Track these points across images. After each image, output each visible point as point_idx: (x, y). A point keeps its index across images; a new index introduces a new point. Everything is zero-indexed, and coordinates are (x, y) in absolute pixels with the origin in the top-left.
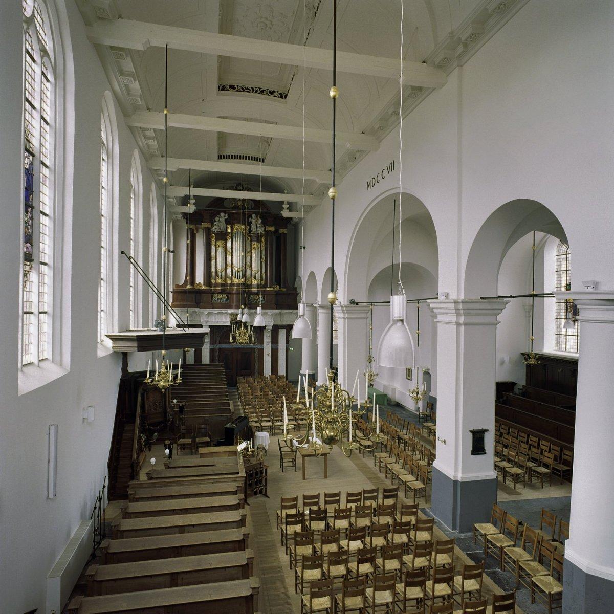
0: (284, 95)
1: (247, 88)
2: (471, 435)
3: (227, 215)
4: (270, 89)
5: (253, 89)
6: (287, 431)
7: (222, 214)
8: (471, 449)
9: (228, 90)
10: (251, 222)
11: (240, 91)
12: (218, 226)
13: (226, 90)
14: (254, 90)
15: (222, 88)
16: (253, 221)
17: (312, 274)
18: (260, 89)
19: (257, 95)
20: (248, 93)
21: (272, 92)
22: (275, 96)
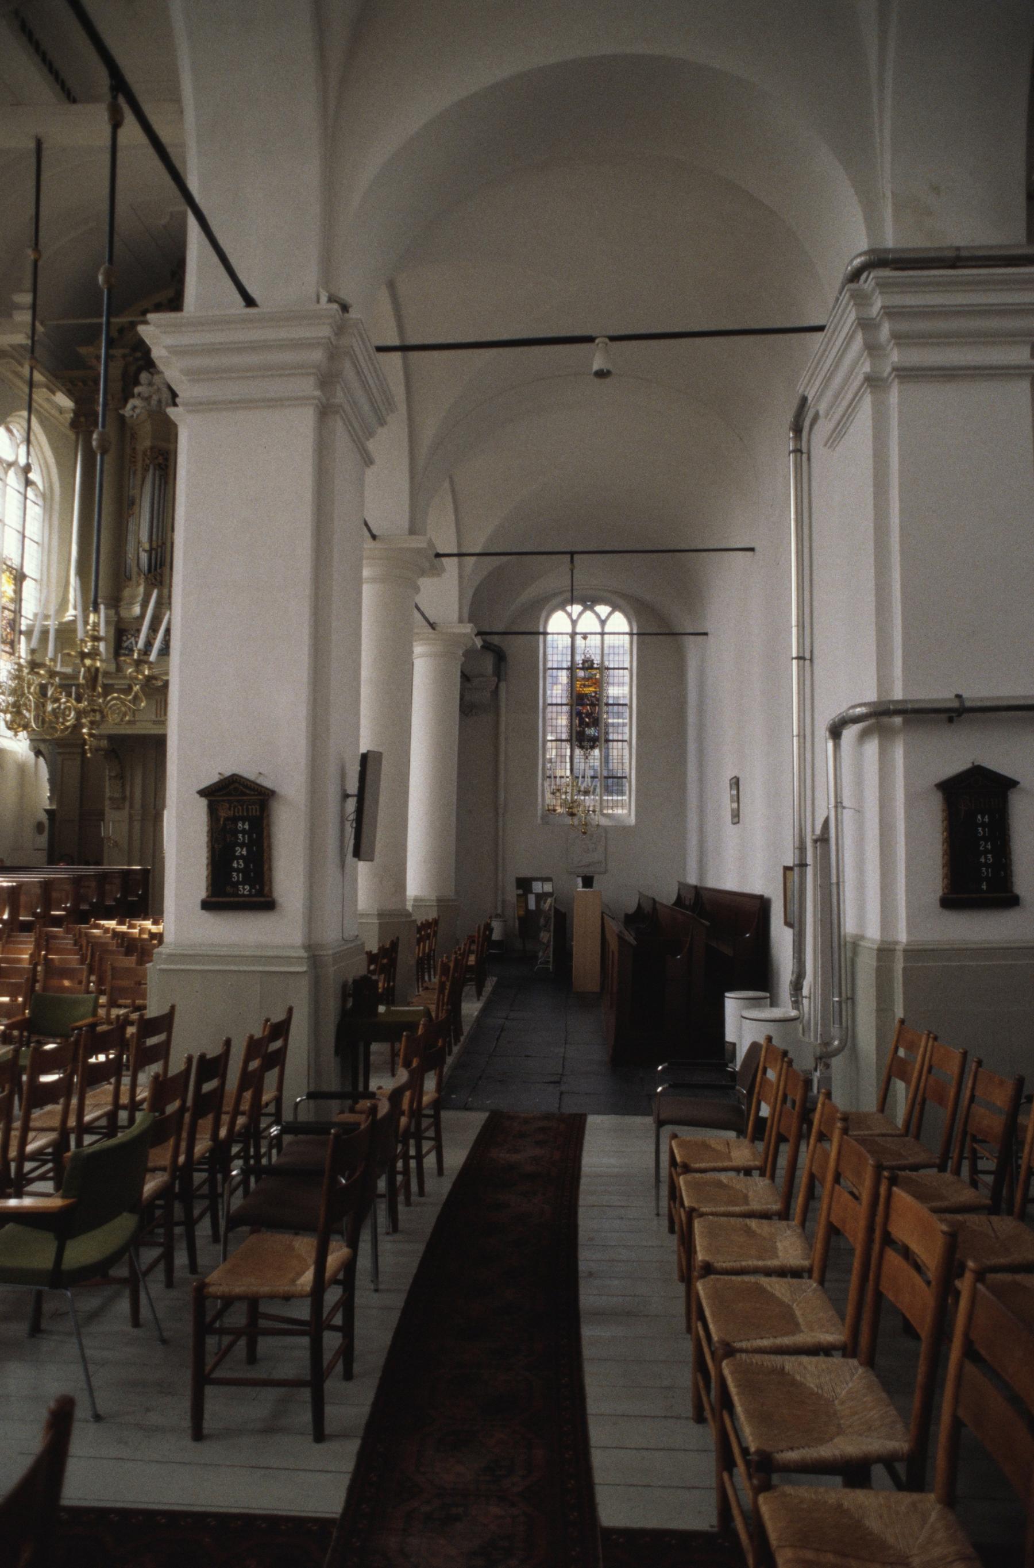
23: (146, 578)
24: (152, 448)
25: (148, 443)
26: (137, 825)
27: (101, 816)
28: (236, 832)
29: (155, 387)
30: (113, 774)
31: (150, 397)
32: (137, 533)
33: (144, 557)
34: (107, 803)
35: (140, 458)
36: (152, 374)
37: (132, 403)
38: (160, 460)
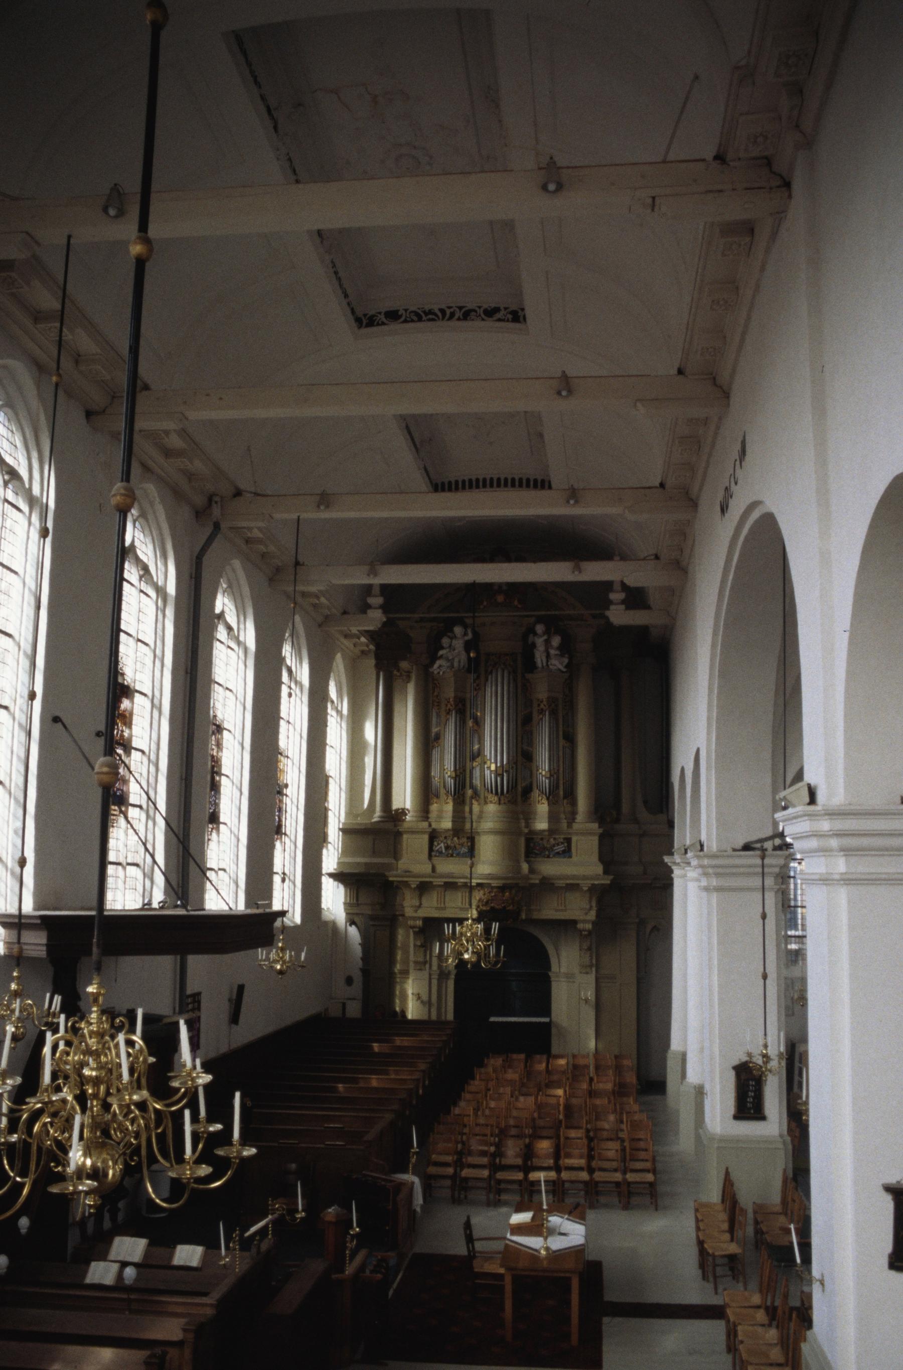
0: (520, 313)
1: (430, 312)
2: (887, 1204)
3: (469, 632)
4: (485, 306)
5: (443, 311)
6: (55, 1076)
7: (458, 630)
8: (887, 1244)
9: (383, 324)
10: (534, 645)
11: (412, 321)
12: (448, 660)
13: (378, 324)
14: (446, 314)
15: (365, 321)
16: (540, 642)
17: (683, 769)
18: (460, 308)
19: (454, 323)
20: (430, 324)
21: (490, 313)
22: (499, 320)
23: (454, 800)
26: (435, 982)
28: (748, 1086)
30: (419, 943)
31: (453, 659)
32: (442, 759)
33: (450, 782)
34: (412, 964)
36: (451, 638)
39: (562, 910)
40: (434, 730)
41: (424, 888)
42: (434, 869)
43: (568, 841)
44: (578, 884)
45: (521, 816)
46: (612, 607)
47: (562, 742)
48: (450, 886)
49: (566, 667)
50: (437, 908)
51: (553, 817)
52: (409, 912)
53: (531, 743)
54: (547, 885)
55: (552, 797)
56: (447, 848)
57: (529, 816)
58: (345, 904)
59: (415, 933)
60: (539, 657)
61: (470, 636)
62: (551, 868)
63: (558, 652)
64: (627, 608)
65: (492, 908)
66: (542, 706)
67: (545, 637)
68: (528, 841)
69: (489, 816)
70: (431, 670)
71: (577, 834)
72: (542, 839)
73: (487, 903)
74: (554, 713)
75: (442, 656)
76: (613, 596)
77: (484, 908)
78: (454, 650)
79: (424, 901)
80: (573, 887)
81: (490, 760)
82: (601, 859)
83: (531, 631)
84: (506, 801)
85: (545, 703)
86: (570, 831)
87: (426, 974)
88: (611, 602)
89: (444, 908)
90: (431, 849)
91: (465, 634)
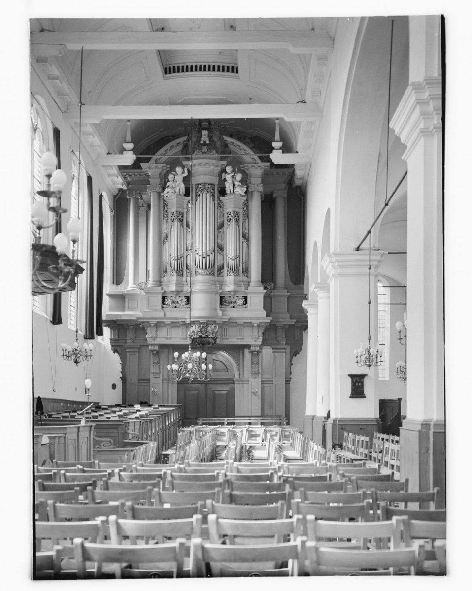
7: (179, 170)
10: (225, 180)
16: (228, 177)
24: (177, 211)
25: (175, 209)
27: (148, 380)
29: (178, 183)
32: (170, 248)
35: (170, 215)
37: (166, 190)
38: (180, 217)
39: (242, 339)
40: (165, 231)
41: (158, 325)
42: (165, 315)
43: (246, 298)
44: (251, 322)
45: (218, 283)
46: (274, 151)
47: (242, 239)
48: (174, 324)
49: (246, 192)
50: (167, 339)
51: (236, 283)
52: (150, 341)
53: (223, 240)
54: (232, 323)
55: (236, 270)
56: (173, 302)
57: (222, 284)
58: (111, 339)
59: (153, 354)
60: (228, 186)
61: (186, 174)
62: (233, 313)
63: (240, 184)
64: (283, 153)
65: (200, 336)
66: (230, 217)
67: (232, 174)
68: (222, 298)
69: (199, 283)
70: (162, 194)
71: (250, 293)
72: (230, 297)
73: (197, 333)
74: (237, 221)
75: (169, 186)
76: (274, 144)
77: (195, 337)
78: (176, 182)
79: (158, 332)
80: (249, 324)
81: (199, 249)
82: (265, 308)
83: (224, 171)
84: (208, 273)
85: (232, 215)
86: (247, 291)
87: (160, 380)
88: (274, 148)
89: (171, 338)
90: (163, 303)
91: (183, 173)
